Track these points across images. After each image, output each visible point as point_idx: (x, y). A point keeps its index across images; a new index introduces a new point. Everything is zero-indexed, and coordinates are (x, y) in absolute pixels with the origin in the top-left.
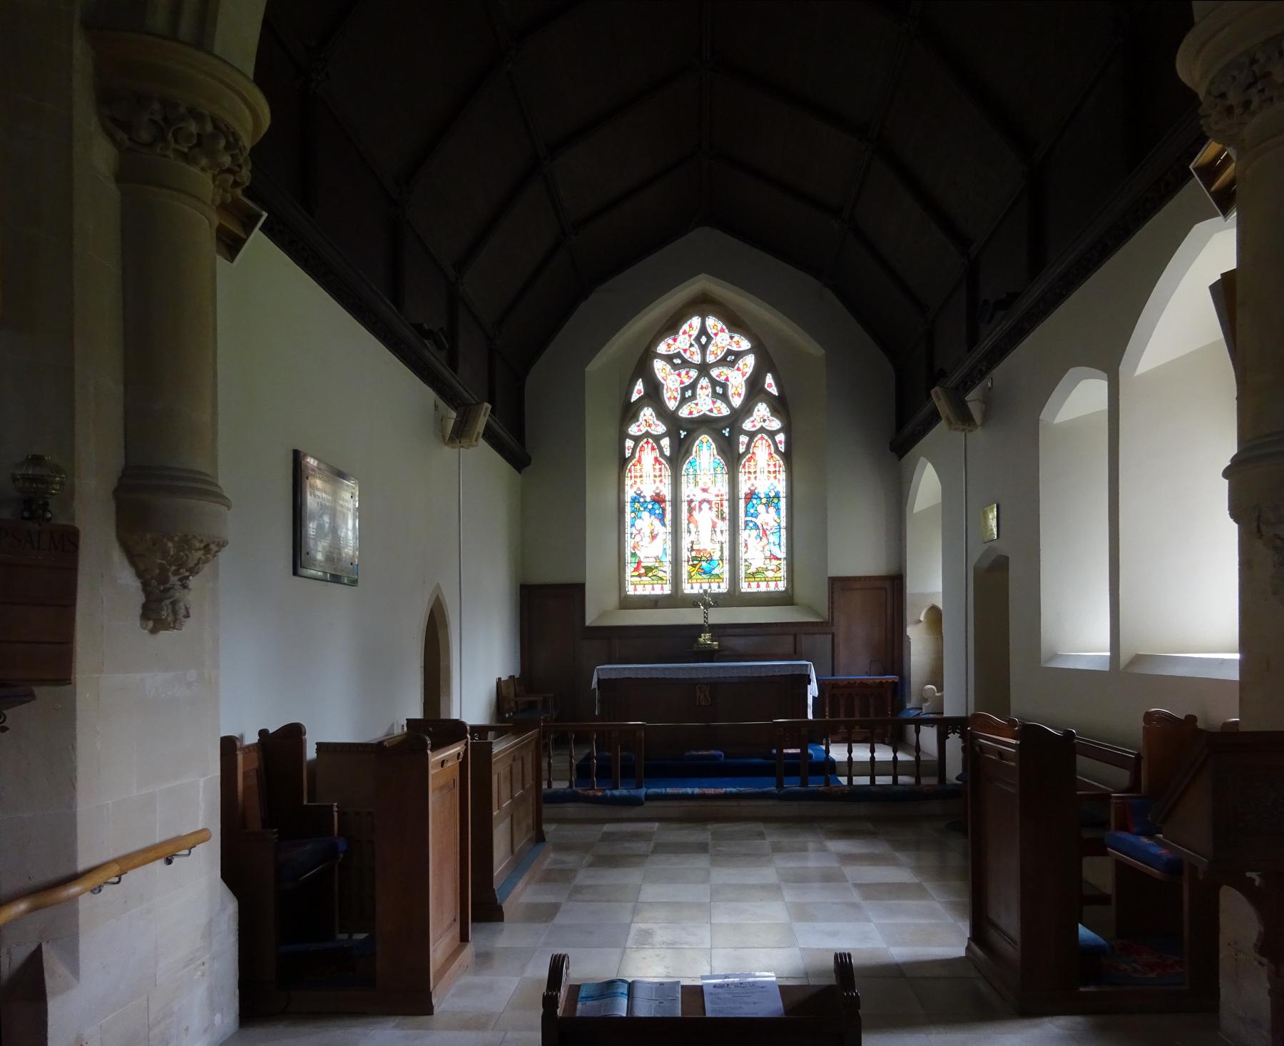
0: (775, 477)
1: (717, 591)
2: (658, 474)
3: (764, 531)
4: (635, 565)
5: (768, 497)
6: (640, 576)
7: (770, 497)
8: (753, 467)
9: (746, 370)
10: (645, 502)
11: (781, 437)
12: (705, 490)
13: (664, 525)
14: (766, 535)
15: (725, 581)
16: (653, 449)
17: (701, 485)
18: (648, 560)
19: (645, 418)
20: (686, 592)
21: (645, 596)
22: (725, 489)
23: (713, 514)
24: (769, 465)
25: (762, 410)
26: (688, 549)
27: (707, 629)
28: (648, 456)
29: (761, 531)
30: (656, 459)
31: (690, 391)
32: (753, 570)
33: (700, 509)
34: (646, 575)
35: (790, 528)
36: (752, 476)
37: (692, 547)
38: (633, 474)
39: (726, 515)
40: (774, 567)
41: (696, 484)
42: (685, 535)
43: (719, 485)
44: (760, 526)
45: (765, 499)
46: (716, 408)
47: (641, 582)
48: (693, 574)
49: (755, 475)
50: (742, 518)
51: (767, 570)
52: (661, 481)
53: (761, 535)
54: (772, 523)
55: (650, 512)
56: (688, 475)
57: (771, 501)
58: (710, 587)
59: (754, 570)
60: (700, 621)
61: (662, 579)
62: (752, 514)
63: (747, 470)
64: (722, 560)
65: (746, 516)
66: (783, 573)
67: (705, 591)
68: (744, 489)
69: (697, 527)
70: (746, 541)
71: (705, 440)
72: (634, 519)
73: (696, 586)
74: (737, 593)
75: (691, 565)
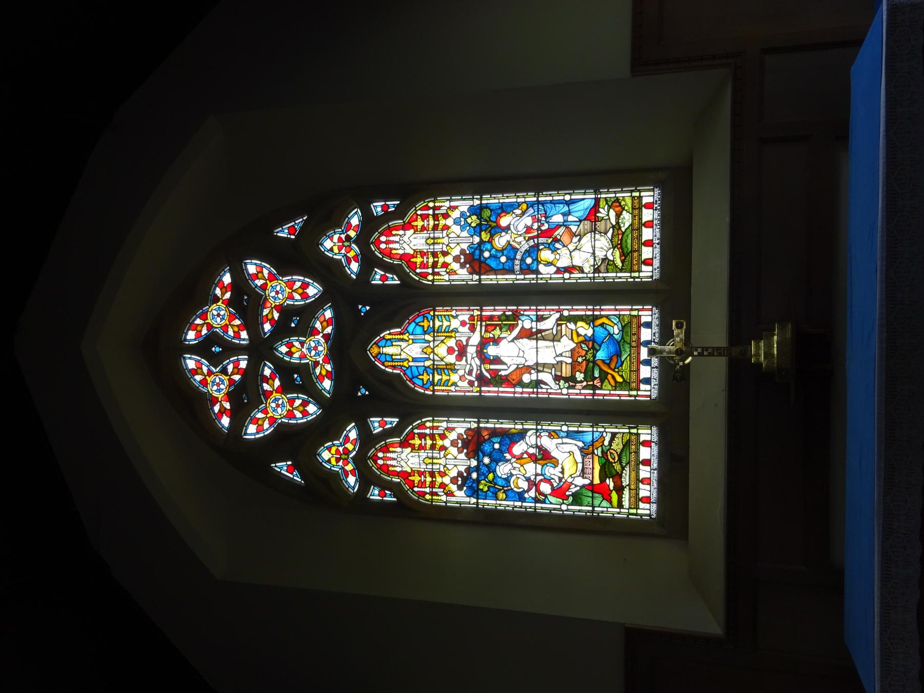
1: (656, 329)
2: (429, 442)
5: (478, 230)
6: (619, 489)
7: (480, 225)
10: (477, 469)
11: (377, 208)
12: (462, 351)
13: (522, 434)
16: (386, 449)
17: (451, 359)
19: (333, 461)
20: (655, 394)
21: (660, 481)
24: (423, 228)
25: (330, 244)
26: (569, 387)
29: (541, 240)
30: (404, 444)
33: (497, 360)
34: (618, 477)
37: (566, 380)
38: (427, 490)
40: (612, 214)
41: (451, 368)
43: (455, 323)
44: (531, 243)
45: (483, 233)
46: (323, 329)
47: (632, 487)
48: (619, 379)
50: (518, 278)
53: (550, 240)
54: (528, 221)
56: (433, 384)
58: (647, 343)
60: (720, 364)
61: (627, 445)
62: (508, 259)
63: (430, 271)
64: (595, 318)
65: (511, 271)
66: (626, 197)
68: (463, 275)
69: (528, 369)
70: (558, 271)
71: (375, 350)
72: (510, 494)
73: (645, 372)
75: (602, 382)
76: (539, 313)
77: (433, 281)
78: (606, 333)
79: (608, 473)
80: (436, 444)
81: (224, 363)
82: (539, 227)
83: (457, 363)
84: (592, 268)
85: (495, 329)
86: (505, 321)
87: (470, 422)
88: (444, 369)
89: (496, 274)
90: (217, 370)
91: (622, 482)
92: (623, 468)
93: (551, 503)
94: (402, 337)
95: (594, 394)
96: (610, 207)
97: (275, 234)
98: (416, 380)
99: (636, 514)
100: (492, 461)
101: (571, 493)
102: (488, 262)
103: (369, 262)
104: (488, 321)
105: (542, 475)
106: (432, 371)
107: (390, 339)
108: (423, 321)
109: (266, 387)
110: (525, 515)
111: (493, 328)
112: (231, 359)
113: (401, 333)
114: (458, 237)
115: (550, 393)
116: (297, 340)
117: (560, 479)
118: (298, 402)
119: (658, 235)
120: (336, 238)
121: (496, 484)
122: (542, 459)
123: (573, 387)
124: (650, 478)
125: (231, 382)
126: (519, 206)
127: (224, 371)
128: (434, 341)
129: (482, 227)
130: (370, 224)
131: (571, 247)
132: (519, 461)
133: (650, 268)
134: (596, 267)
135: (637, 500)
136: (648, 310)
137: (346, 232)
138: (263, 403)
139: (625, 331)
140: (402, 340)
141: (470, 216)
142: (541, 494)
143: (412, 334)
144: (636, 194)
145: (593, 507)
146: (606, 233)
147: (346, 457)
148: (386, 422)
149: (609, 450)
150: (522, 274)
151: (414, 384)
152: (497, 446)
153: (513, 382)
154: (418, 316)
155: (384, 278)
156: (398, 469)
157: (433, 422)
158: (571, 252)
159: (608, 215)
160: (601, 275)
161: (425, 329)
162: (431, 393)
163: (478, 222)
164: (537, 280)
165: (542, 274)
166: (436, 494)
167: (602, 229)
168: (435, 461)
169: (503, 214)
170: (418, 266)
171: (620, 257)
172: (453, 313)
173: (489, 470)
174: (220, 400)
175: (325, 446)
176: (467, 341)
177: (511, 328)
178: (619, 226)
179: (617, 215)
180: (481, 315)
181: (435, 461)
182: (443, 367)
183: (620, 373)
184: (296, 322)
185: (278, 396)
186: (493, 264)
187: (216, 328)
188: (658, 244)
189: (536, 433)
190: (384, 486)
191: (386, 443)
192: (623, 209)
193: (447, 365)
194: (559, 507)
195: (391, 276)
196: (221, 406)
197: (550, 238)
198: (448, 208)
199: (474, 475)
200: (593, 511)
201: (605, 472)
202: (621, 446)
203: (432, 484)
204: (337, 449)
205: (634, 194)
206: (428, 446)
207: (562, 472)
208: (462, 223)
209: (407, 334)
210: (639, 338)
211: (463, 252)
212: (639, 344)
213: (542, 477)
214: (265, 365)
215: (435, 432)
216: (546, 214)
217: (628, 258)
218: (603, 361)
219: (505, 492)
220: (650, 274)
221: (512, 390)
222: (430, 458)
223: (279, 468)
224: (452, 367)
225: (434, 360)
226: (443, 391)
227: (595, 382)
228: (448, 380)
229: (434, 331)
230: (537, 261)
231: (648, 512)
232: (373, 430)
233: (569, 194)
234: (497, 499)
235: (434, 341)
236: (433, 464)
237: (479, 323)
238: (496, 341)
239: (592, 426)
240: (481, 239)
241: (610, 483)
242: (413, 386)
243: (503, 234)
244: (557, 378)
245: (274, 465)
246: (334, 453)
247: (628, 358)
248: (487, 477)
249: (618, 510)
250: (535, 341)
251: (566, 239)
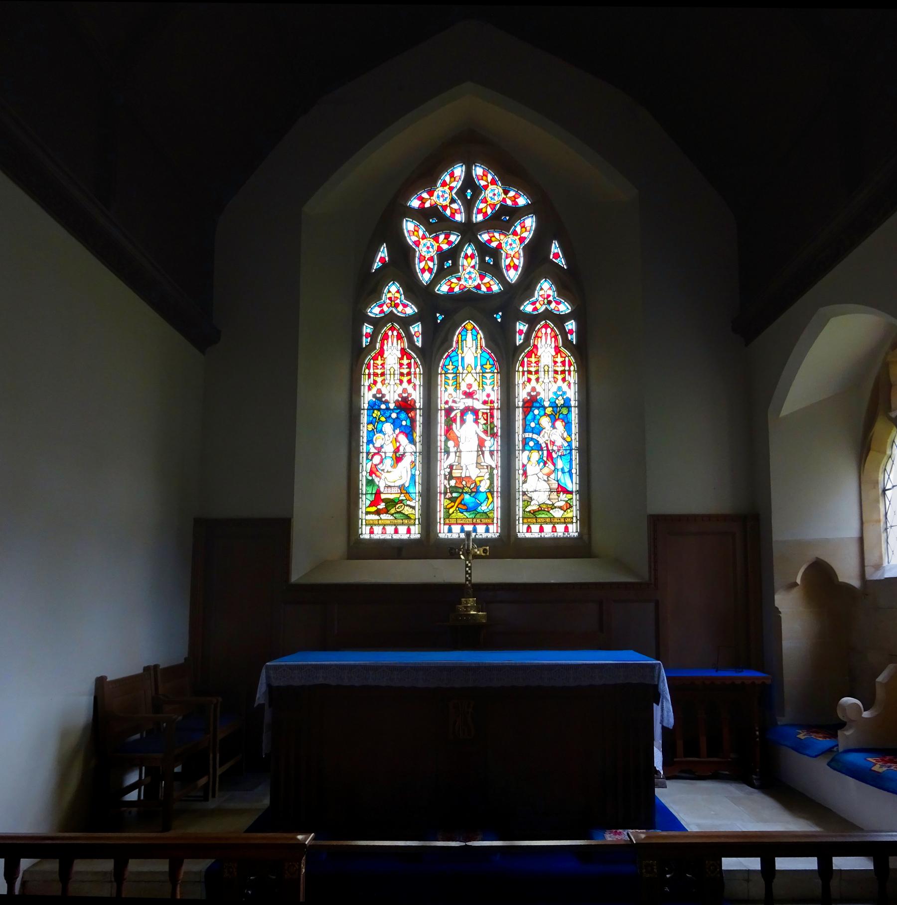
0: (564, 380)
1: (485, 535)
2: (405, 371)
3: (549, 455)
4: (372, 498)
5: (554, 406)
6: (378, 512)
7: (557, 406)
8: (533, 365)
9: (525, 235)
10: (388, 409)
11: (571, 325)
12: (469, 395)
13: (412, 441)
14: (552, 458)
15: (495, 521)
16: (399, 337)
17: (464, 387)
18: (389, 490)
19: (389, 295)
20: (441, 536)
21: (384, 541)
22: (495, 395)
23: (480, 429)
24: (555, 362)
25: (546, 288)
26: (445, 476)
27: (471, 591)
28: (392, 351)
29: (545, 453)
30: (403, 351)
31: (450, 262)
32: (533, 507)
33: (463, 421)
35: (585, 451)
36: (533, 377)
37: (450, 473)
39: (498, 430)
40: (562, 504)
41: (457, 387)
42: (441, 456)
43: (488, 389)
44: (544, 445)
45: (551, 409)
46: (485, 284)
47: (380, 522)
48: (451, 511)
49: (536, 376)
50: (519, 435)
51: (553, 507)
52: (409, 382)
53: (545, 459)
54: (559, 442)
55: (393, 423)
56: (446, 373)
57: (558, 413)
58: (475, 530)
59: (536, 508)
60: (460, 579)
61: (408, 517)
63: (526, 369)
64: (492, 493)
65: (524, 431)
66: (573, 513)
67: (468, 534)
68: (522, 394)
69: (457, 445)
70: (524, 466)
71: (469, 327)
73: (456, 529)
74: (512, 539)
75: (449, 499)
76: (495, 452)
77: (518, 371)
78: (482, 501)
79: (388, 504)
80: (404, 376)
81: (459, 201)
82: (554, 451)
83: (461, 391)
84: (526, 490)
85: (485, 419)
86: (490, 427)
87: (420, 402)
88: (457, 381)
89: (523, 419)
90: (454, 195)
91: (383, 514)
92: (392, 515)
93: (367, 464)
94: (479, 347)
95: (441, 493)
96: (567, 502)
97: (554, 242)
98: (448, 359)
99: (362, 524)
100: (394, 419)
101: (374, 478)
102: (531, 413)
103: (532, 320)
104: (490, 415)
105: (385, 457)
106: (455, 372)
107: (477, 338)
108: (490, 364)
109: (442, 237)
110: (358, 445)
111: (486, 418)
112: (462, 207)
113: (481, 347)
114: (549, 390)
115: (441, 462)
116: (476, 263)
117: (383, 470)
118: (431, 264)
119: (546, 536)
120: (550, 292)
121: (378, 423)
122: (396, 457)
123: (445, 478)
124: (386, 533)
125: (445, 208)
126: (569, 436)
127: (453, 201)
128: (476, 373)
129: (555, 408)
130: (559, 320)
131: (540, 475)
132: (394, 440)
133: (525, 530)
134: (527, 493)
135: (372, 525)
136: (497, 530)
137: (554, 301)
138: (430, 235)
139: (484, 514)
140: (477, 348)
141: (563, 398)
142: (373, 457)
143: (481, 356)
144: (574, 520)
145: (366, 494)
146: (549, 499)
147: (393, 305)
148: (419, 336)
149: (404, 504)
150: (523, 439)
151: (446, 358)
152: (404, 423)
153: (448, 434)
154: (494, 360)
155: (521, 332)
156: (385, 347)
157: (419, 374)
158: (536, 474)
159: (561, 500)
160: (521, 496)
161: (484, 366)
162: (440, 372)
163: (559, 405)
164: (518, 450)
165: (522, 453)
166: (369, 377)
167: (551, 497)
168: (392, 376)
169: (564, 423)
170: (529, 359)
171: (533, 510)
172: (496, 388)
173: (387, 417)
174: (431, 198)
175: (400, 288)
176: (476, 399)
177: (485, 432)
178: (554, 509)
179: (561, 507)
180: (494, 409)
181: (392, 376)
182: (458, 380)
183: (455, 512)
184: (489, 261)
185: (436, 248)
186: (530, 417)
187: (485, 193)
188: (541, 536)
189: (414, 452)
190: (373, 336)
191: (404, 337)
192: (565, 511)
193: (460, 383)
194: (365, 470)
195: (522, 339)
196: (427, 199)
197: (547, 459)
198: (569, 382)
199: (383, 407)
200: (362, 494)
201: (389, 502)
202: (406, 513)
203: (376, 375)
204: (397, 298)
205: (574, 518)
206: (402, 371)
207: (388, 472)
208: (558, 393)
209: (481, 352)
210: (478, 524)
211: (538, 394)
212: (474, 524)
213: (384, 457)
214: (458, 236)
215: (413, 376)
216: (563, 455)
217: (532, 516)
218: (463, 499)
219: (373, 429)
220: (521, 531)
221: (443, 434)
222: (394, 372)
223: (383, 250)
224: (458, 388)
225: (462, 373)
226: (441, 381)
227: (449, 494)
228: (449, 385)
229: (483, 373)
230: (532, 449)
231: (364, 533)
232: (413, 326)
233: (576, 472)
234: (368, 424)
235: (476, 373)
236: (390, 374)
237: (489, 408)
238: (476, 421)
239: (419, 492)
240: (547, 407)
241: (382, 506)
242: (444, 358)
243: (550, 424)
244: (451, 467)
245: (385, 246)
246: (395, 296)
247: (465, 517)
248: (382, 416)
249: (364, 512)
250: (476, 450)
251: (546, 470)
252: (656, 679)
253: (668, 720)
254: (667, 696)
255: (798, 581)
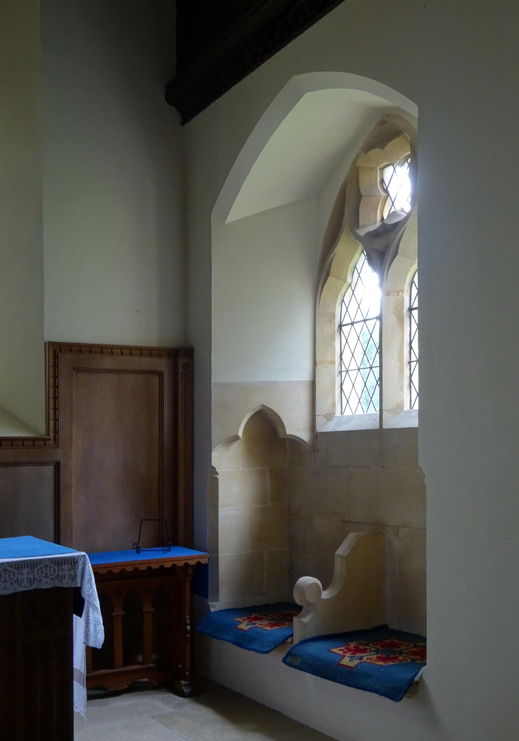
252: (79, 579)
253: (96, 637)
254: (95, 603)
255: (240, 434)
